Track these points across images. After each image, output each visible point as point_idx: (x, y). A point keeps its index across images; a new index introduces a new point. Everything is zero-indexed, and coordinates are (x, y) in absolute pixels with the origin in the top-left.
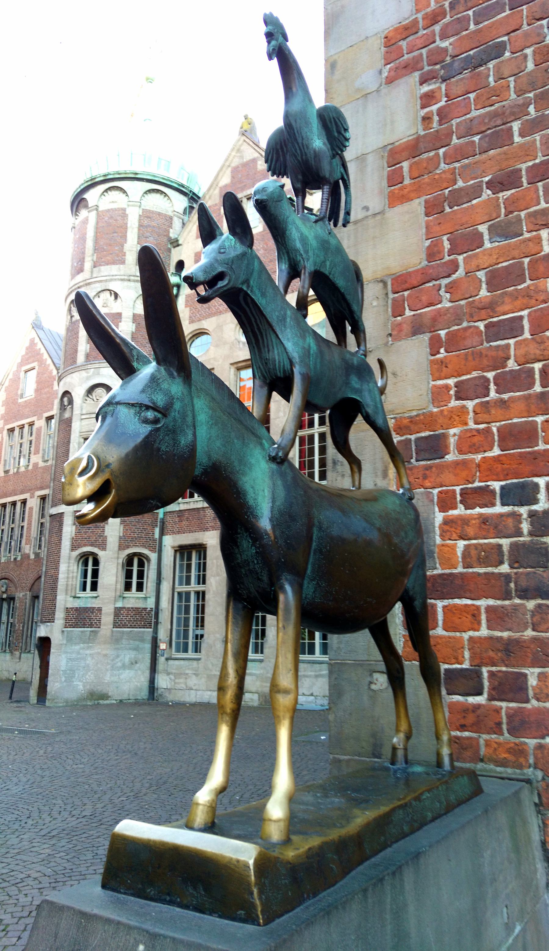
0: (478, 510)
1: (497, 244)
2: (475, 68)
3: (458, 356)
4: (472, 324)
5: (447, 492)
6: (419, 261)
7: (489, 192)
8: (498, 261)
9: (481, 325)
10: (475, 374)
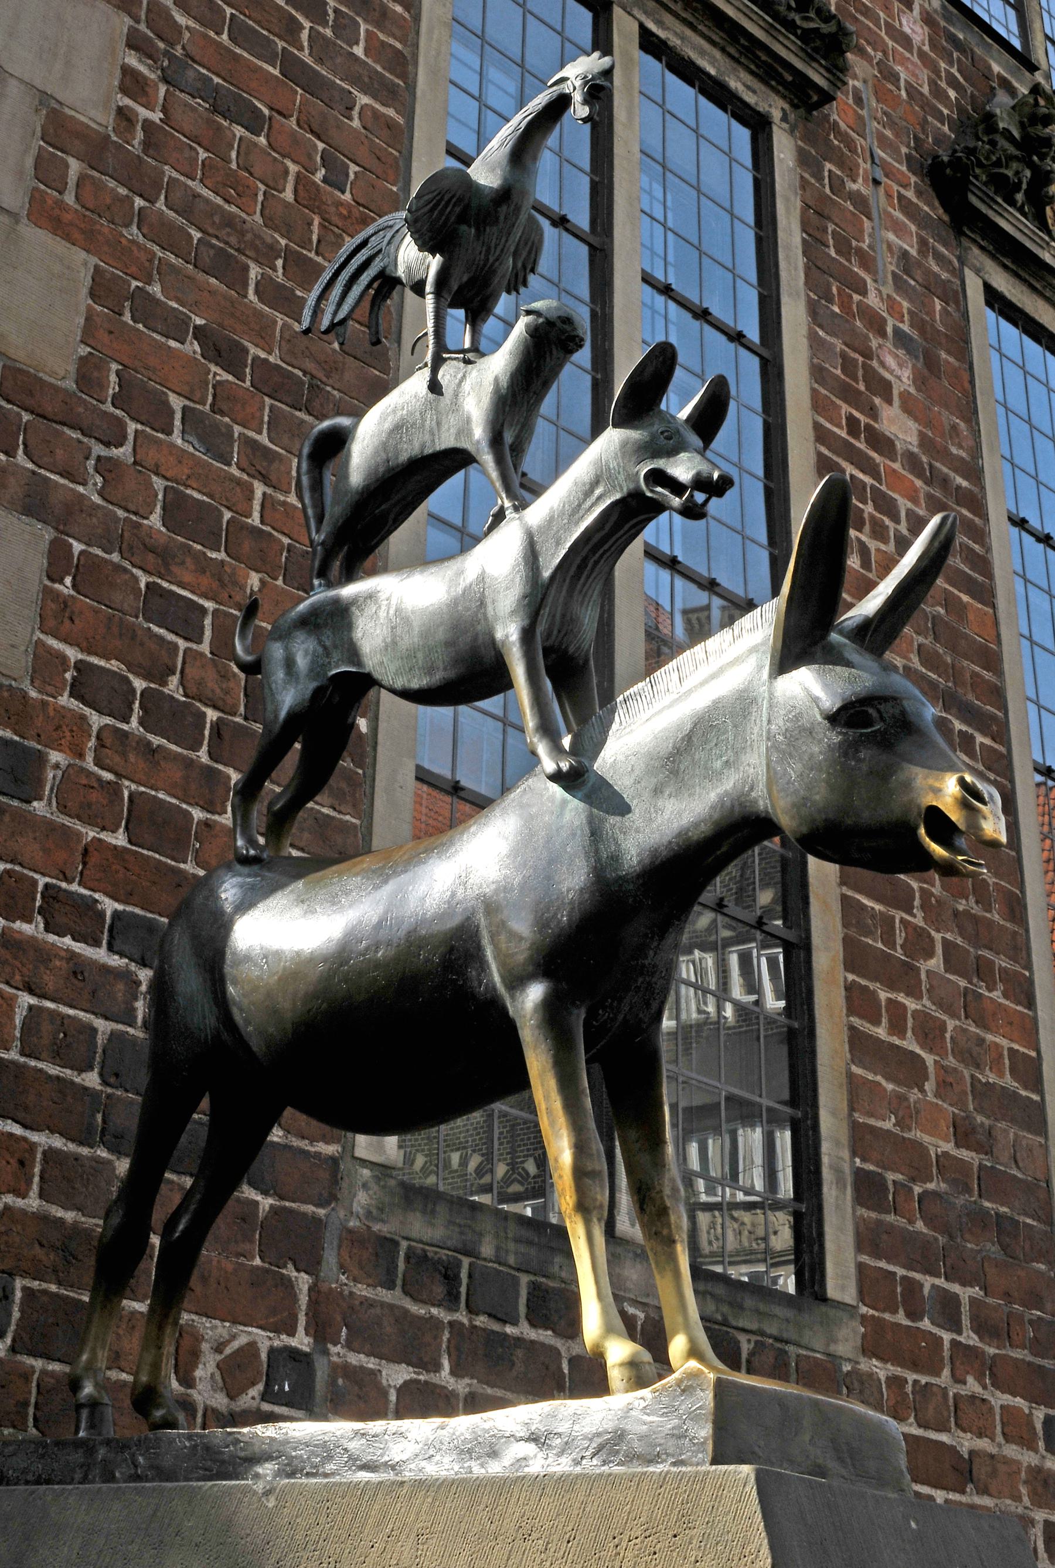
1: (191, 449)
2: (215, 109)
3: (97, 611)
4: (127, 564)
6: (62, 373)
7: (198, 348)
8: (189, 482)
9: (143, 580)
10: (114, 665)
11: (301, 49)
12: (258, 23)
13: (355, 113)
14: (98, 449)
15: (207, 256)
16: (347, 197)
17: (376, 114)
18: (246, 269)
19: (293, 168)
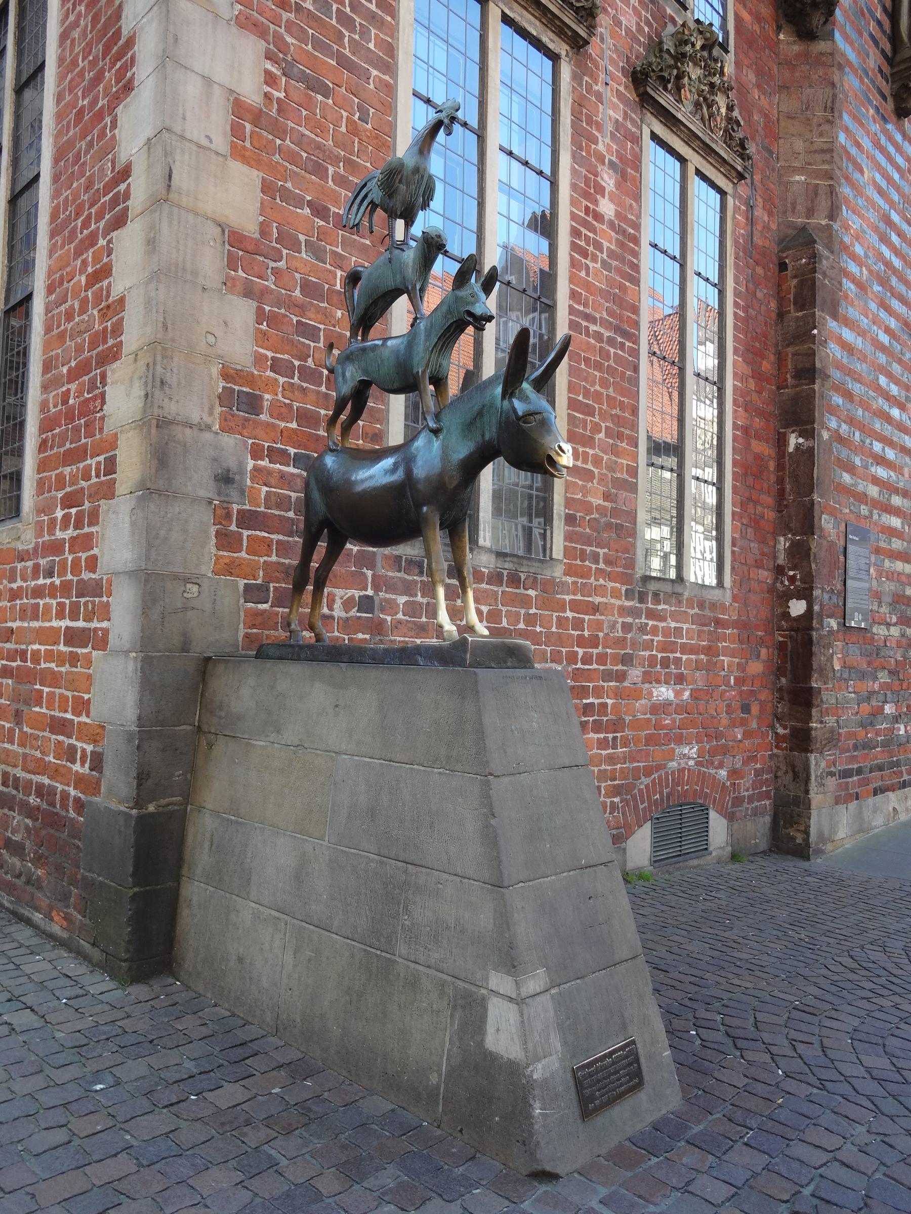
0: (278, 465)
3: (277, 335)
5: (258, 445)
9: (295, 319)
10: (286, 357)
11: (345, 49)
12: (324, 36)
13: (371, 81)
14: (272, 264)
15: (310, 165)
16: (369, 126)
17: (380, 78)
18: (327, 169)
19: (345, 114)
